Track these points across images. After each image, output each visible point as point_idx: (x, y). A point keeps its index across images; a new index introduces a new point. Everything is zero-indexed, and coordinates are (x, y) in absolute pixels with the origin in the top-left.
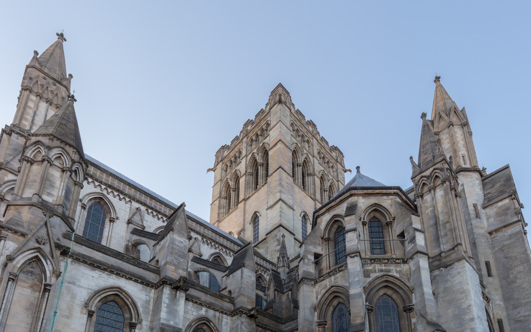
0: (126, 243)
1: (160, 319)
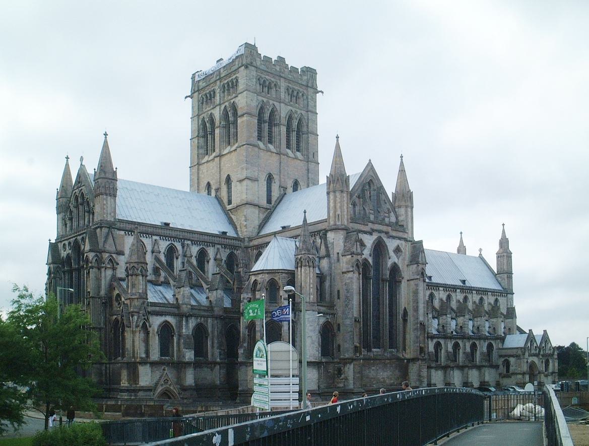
0: (153, 266)
1: (183, 333)
